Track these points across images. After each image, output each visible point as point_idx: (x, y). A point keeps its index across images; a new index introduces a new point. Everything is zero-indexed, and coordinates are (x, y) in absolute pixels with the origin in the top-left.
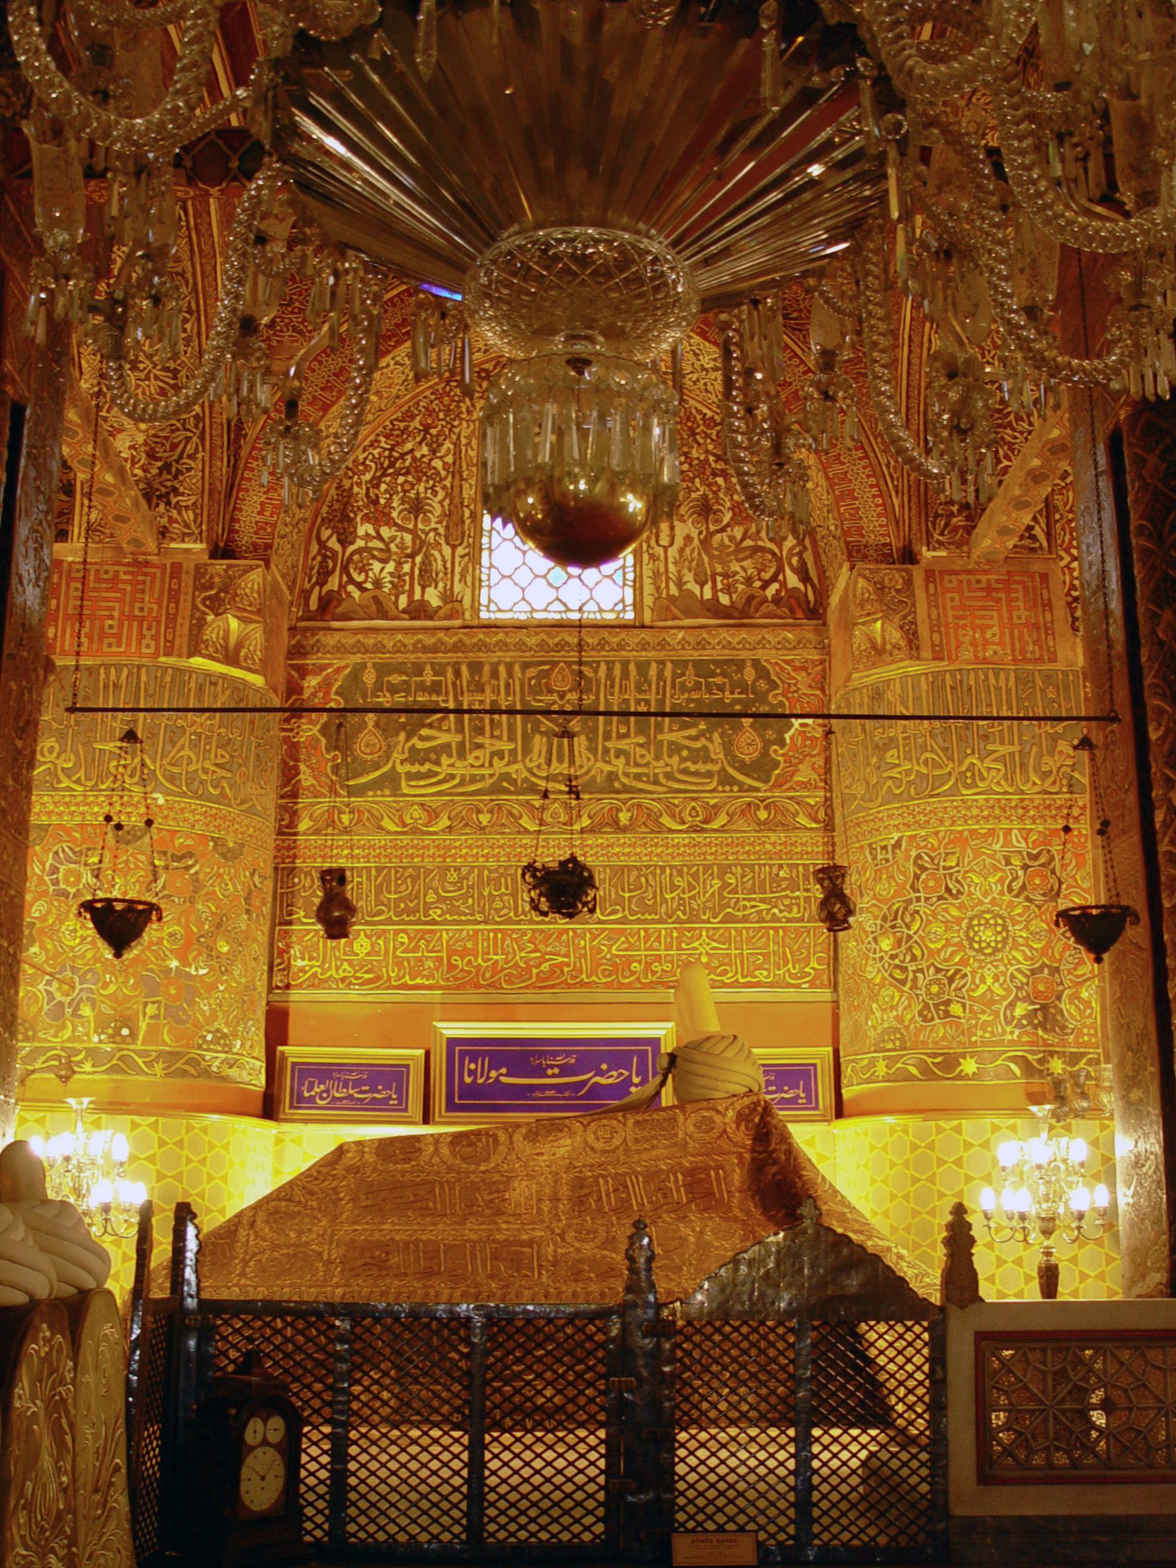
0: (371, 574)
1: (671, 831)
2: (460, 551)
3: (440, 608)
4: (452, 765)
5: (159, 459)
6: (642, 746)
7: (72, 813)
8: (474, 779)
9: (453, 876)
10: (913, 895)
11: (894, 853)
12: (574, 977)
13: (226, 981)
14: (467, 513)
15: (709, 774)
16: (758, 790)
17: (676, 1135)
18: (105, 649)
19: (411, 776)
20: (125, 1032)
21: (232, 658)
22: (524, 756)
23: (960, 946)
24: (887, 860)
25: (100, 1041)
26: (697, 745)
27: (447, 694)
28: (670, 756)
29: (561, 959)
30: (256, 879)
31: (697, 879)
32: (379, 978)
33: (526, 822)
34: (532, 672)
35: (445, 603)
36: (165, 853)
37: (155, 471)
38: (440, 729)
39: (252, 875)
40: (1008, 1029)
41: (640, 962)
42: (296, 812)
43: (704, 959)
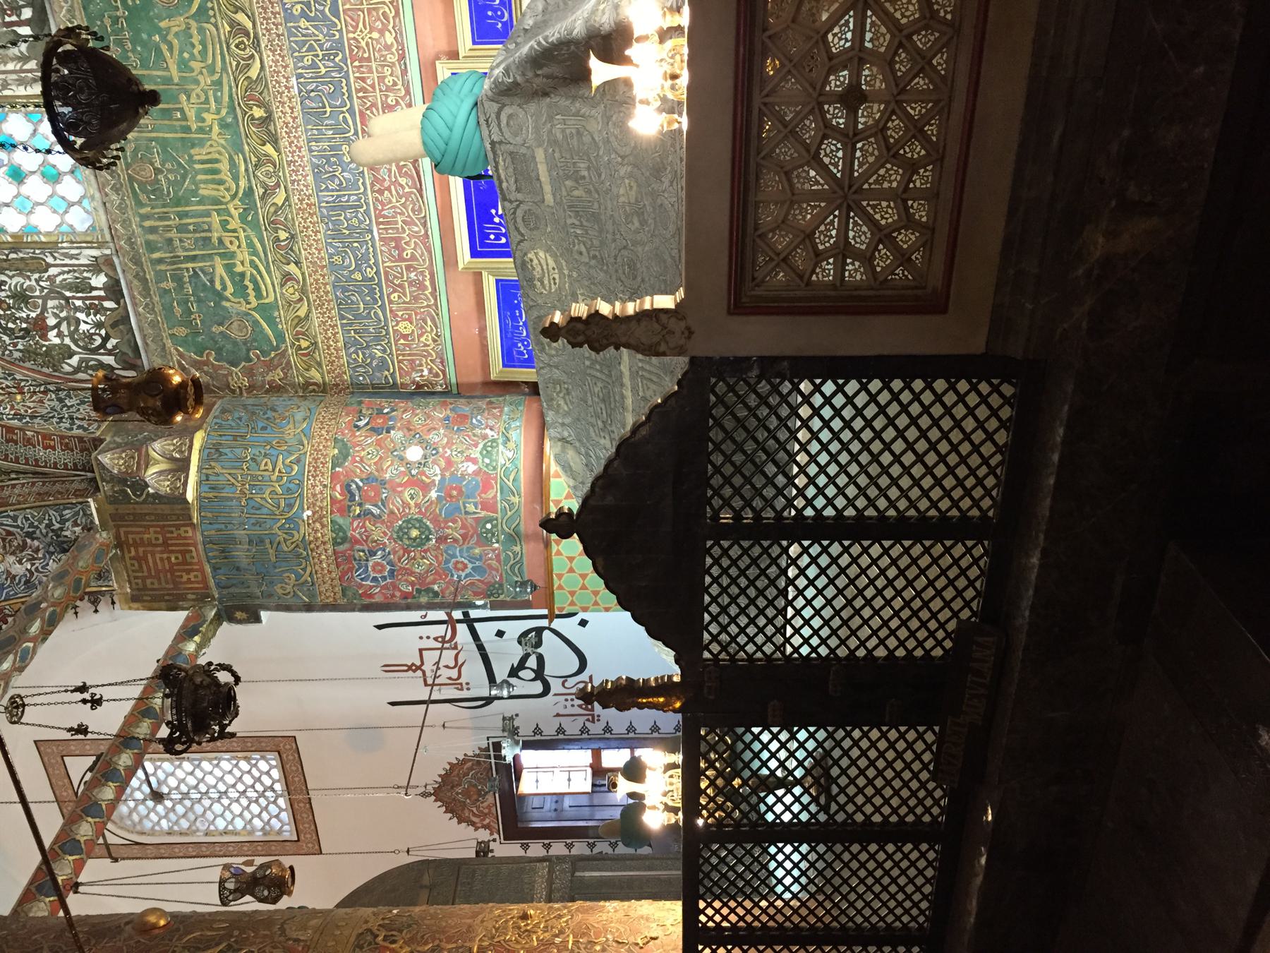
0: (92, 331)
2: (50, 260)
3: (106, 275)
4: (242, 263)
5: (25, 543)
6: (189, 98)
7: (330, 572)
8: (251, 245)
14: (12, 256)
15: (201, 31)
18: (196, 560)
19: (259, 295)
20: (489, 526)
21: (181, 466)
22: (222, 203)
25: (497, 542)
26: (175, 42)
27: (180, 269)
28: (192, 70)
29: (394, 168)
30: (361, 423)
31: (305, 42)
34: (143, 197)
35: (100, 271)
36: (350, 507)
37: (36, 543)
41: (387, 96)
42: (306, 382)
43: (375, 35)
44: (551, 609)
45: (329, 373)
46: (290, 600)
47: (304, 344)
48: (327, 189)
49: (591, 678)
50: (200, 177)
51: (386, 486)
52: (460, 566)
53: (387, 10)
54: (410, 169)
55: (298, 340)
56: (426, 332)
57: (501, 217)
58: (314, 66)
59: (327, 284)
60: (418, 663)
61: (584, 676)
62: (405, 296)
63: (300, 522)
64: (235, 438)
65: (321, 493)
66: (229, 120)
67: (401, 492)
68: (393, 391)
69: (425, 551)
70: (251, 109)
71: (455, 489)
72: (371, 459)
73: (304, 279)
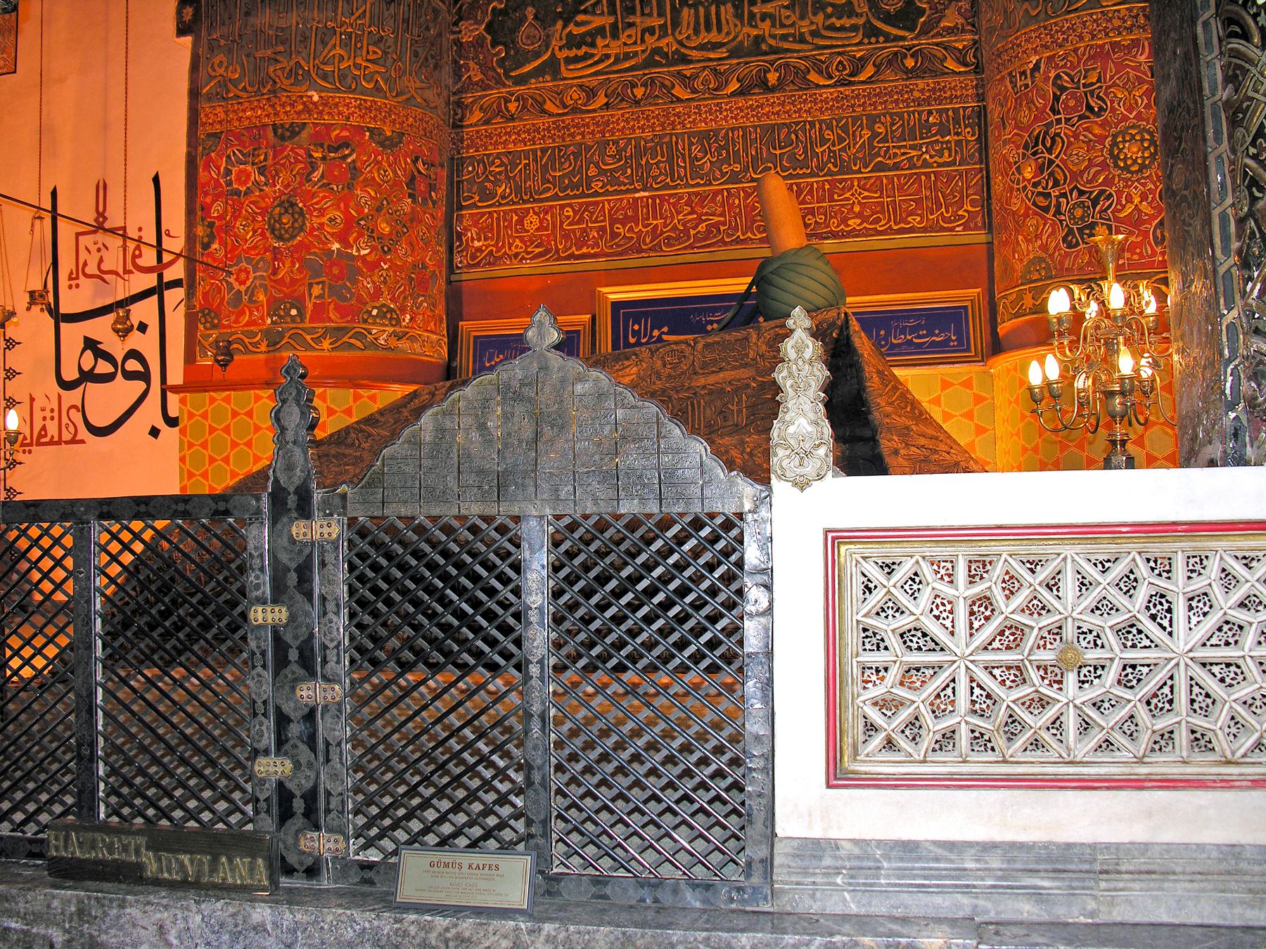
1: (818, 86)
6: (786, 7)
8: (627, 57)
9: (612, 150)
10: (1054, 118)
11: (1032, 76)
12: (729, 236)
13: (390, 260)
15: (854, 28)
16: (903, 38)
17: (747, 355)
19: (569, 61)
22: (674, 30)
23: (1104, 166)
24: (1026, 86)
28: (815, 14)
29: (717, 219)
30: (420, 166)
31: (846, 131)
32: (547, 251)
33: (679, 91)
36: (322, 146)
38: (594, 13)
39: (415, 161)
40: (1159, 250)
44: (176, 389)
45: (477, 132)
46: (202, 73)
47: (512, 107)
48: (691, 144)
49: (82, 442)
50: (701, 10)
51: (346, 191)
52: (243, 276)
53: (883, 222)
54: (715, 236)
55: (517, 100)
56: (527, 247)
57: (660, 340)
58: (823, 141)
59: (583, 136)
60: (107, 225)
61: (83, 433)
62: (569, 224)
63: (304, 88)
64: (406, 21)
65: (340, 113)
66: (764, 47)
67: (339, 207)
68: (454, 206)
69: (263, 234)
70: (776, 70)
71: (341, 272)
72: (379, 174)
73: (589, 111)
